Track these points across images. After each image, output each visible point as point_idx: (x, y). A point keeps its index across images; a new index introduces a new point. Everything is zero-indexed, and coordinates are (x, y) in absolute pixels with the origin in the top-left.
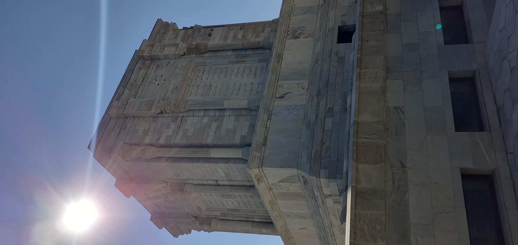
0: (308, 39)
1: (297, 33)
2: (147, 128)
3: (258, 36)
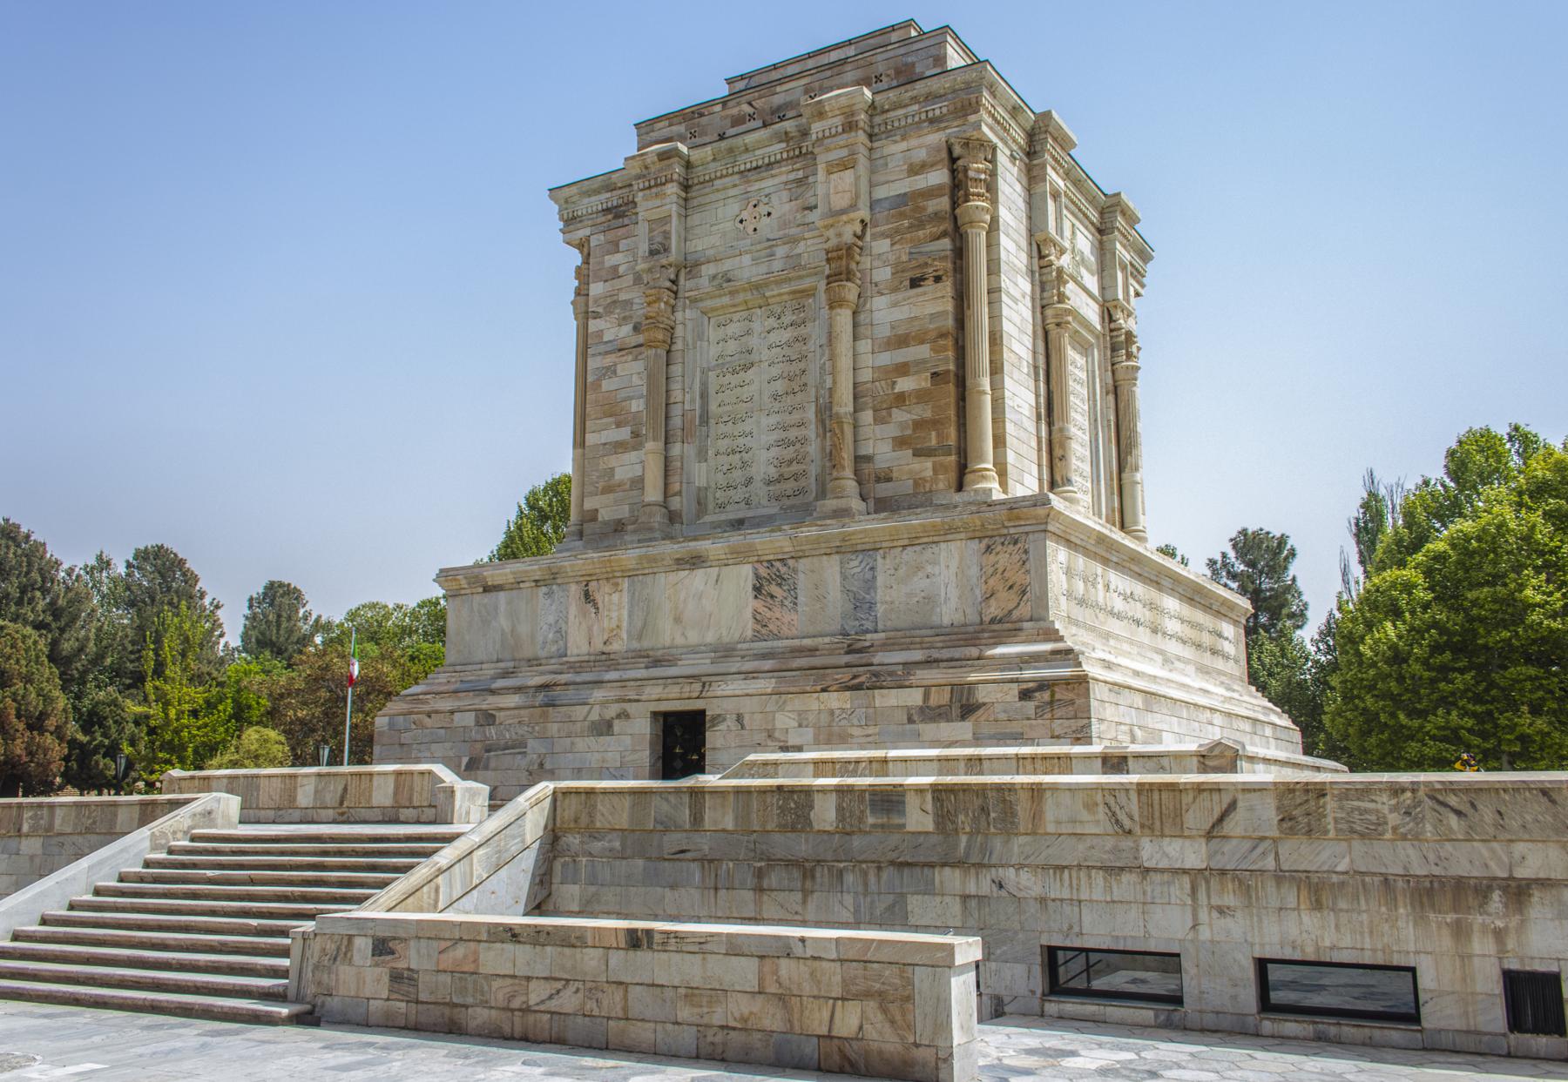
0: (750, 624)
1: (774, 589)
2: (621, 270)
3: (900, 443)
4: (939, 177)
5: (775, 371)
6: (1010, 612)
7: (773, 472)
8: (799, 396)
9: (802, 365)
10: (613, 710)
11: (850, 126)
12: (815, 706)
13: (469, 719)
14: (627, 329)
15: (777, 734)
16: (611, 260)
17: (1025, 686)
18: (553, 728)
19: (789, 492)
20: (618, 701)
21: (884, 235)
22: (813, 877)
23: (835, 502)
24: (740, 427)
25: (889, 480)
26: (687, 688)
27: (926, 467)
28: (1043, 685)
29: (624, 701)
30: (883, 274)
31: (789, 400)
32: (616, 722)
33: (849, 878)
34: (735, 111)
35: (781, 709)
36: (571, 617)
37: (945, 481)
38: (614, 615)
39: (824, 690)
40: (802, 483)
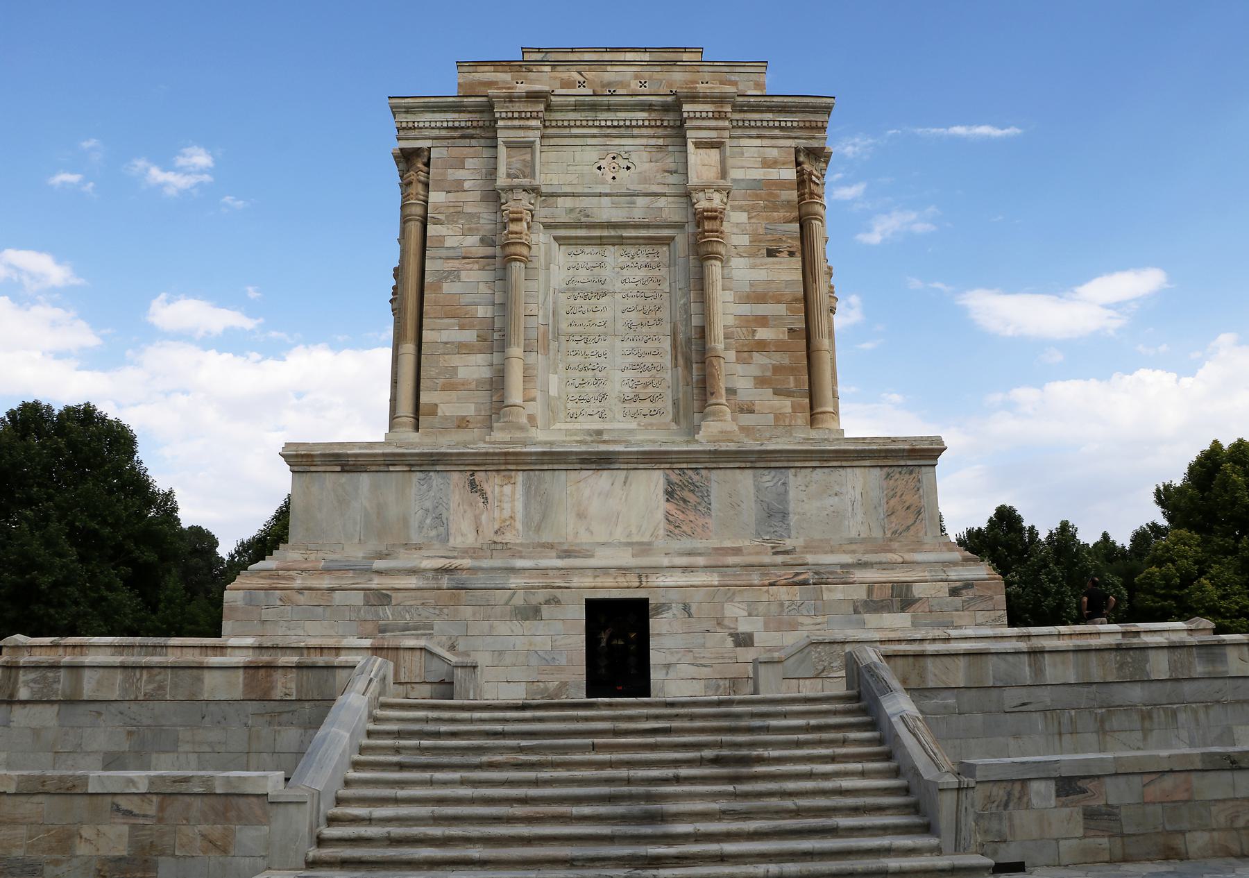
0: (663, 524)
1: (687, 494)
2: (467, 185)
3: (761, 382)
5: (630, 302)
6: (908, 528)
8: (654, 329)
9: (657, 302)
10: (541, 596)
11: (719, 116)
12: (765, 598)
13: (357, 598)
14: (472, 241)
15: (726, 622)
17: (953, 585)
18: (467, 612)
19: (646, 411)
20: (543, 588)
21: (741, 209)
22: (1151, 717)
23: (719, 424)
24: (593, 347)
25: (752, 412)
26: (621, 579)
27: (786, 405)
28: (968, 585)
29: (553, 588)
30: (743, 240)
31: (645, 329)
32: (544, 607)
33: (1182, 717)
34: (565, 76)
35: (730, 600)
36: (453, 505)
37: (802, 418)
38: (507, 506)
39: (771, 585)
40: (659, 404)
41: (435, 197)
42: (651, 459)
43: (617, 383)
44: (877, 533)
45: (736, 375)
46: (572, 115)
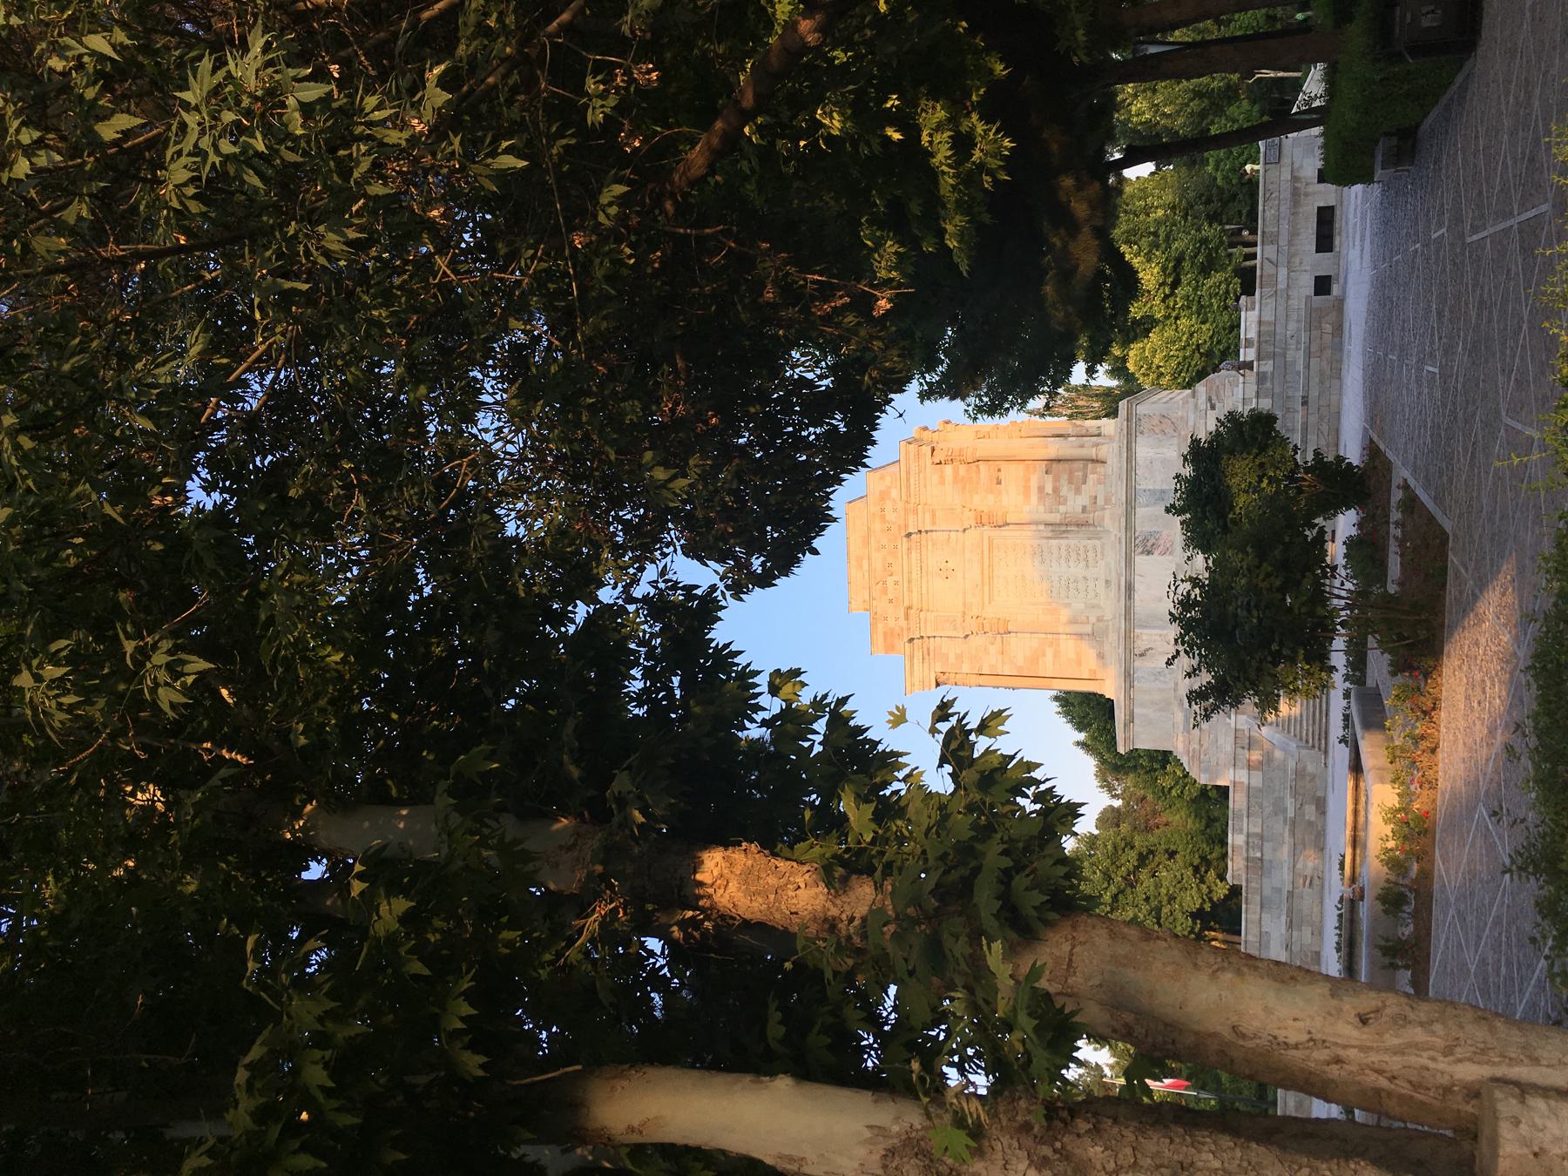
3: (1078, 491)
4: (948, 469)
7: (1083, 563)
11: (916, 512)
16: (952, 659)
27: (1092, 478)
28: (1210, 399)
41: (966, 668)
42: (1129, 562)
43: (1077, 570)
44: (1175, 441)
45: (1075, 504)
46: (915, 594)
